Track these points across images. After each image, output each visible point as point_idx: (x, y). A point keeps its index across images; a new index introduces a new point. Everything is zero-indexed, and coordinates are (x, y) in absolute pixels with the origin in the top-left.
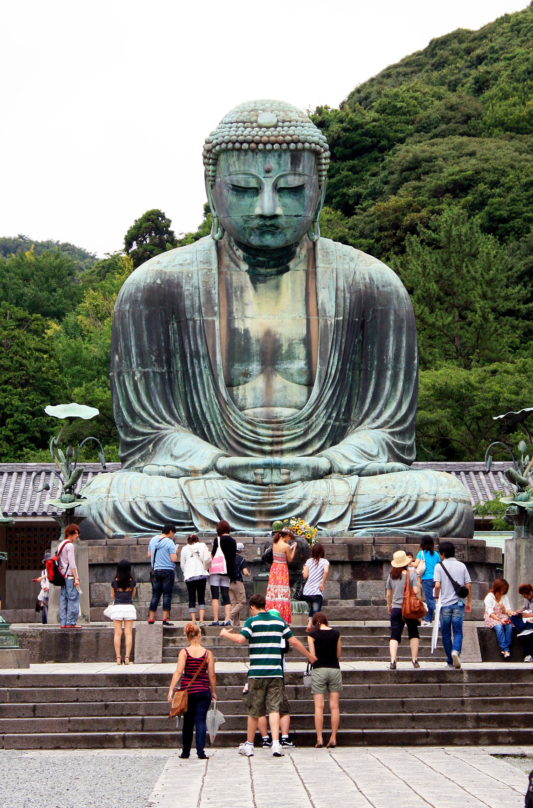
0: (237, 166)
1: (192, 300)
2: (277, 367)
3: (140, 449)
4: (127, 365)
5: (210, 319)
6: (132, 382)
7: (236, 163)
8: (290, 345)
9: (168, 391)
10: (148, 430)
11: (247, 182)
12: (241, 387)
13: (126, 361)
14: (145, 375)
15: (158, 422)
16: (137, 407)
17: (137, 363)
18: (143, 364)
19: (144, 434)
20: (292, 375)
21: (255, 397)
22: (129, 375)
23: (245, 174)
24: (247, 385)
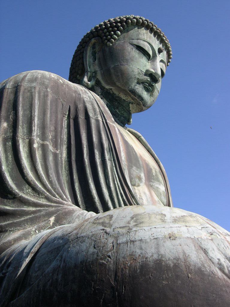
0: (145, 37)
1: (92, 105)
2: (151, 183)
3: (32, 221)
4: (23, 131)
5: (111, 123)
6: (26, 149)
7: (145, 35)
8: (156, 172)
9: (60, 172)
10: (43, 201)
11: (149, 49)
12: (136, 188)
13: (23, 128)
14: (44, 148)
15: (54, 196)
16: (31, 175)
17: (37, 133)
18: (43, 136)
19: (35, 205)
20: (161, 194)
21: (147, 200)
22: (23, 142)
23: (149, 44)
24: (139, 188)
